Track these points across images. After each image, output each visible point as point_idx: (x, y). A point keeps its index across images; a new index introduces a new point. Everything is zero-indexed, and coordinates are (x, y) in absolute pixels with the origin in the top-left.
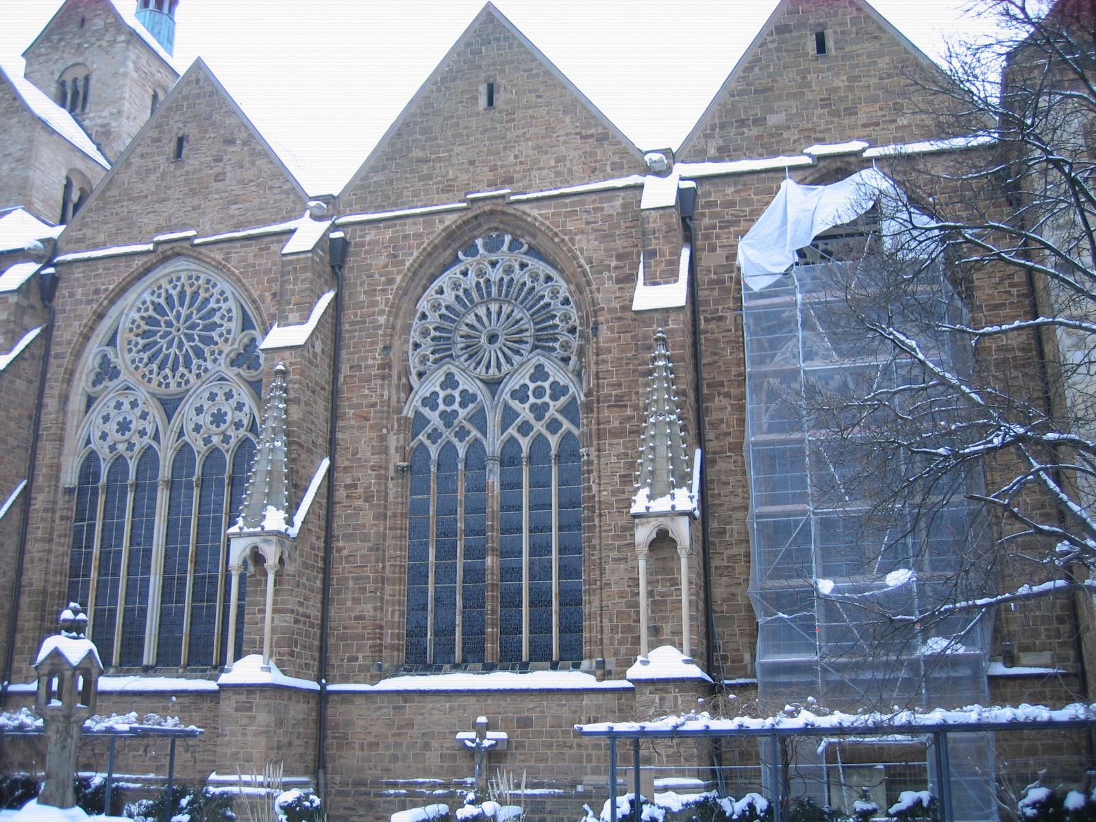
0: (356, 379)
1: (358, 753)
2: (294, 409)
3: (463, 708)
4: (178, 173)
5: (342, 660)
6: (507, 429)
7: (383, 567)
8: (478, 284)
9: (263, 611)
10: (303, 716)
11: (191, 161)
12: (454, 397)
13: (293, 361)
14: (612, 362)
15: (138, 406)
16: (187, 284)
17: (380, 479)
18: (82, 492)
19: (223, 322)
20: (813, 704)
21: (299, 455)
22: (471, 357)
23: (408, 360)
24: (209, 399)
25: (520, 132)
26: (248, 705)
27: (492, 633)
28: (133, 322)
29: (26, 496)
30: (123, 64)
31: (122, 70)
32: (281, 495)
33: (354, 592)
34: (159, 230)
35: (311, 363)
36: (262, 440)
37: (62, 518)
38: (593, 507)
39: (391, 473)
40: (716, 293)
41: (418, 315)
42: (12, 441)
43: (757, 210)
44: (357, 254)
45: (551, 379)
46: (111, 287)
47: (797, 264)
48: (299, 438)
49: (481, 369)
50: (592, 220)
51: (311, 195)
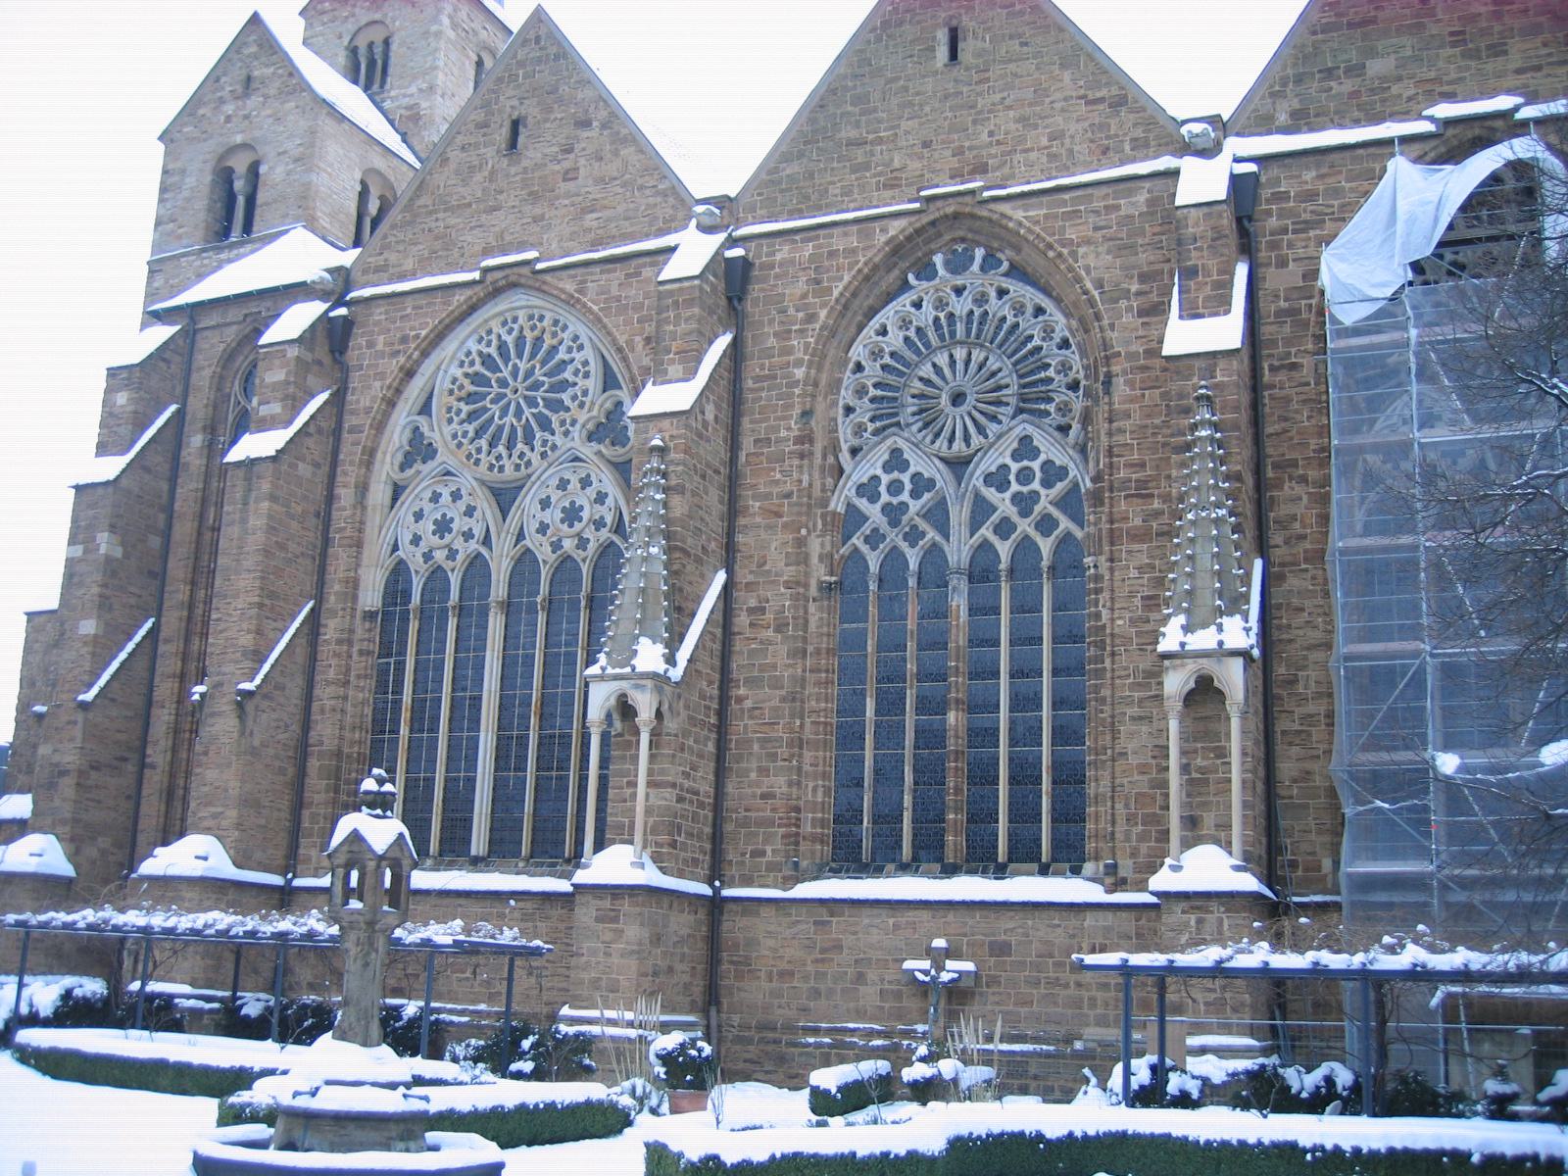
0: (763, 458)
1: (765, 985)
2: (676, 500)
3: (913, 926)
4: (513, 170)
5: (743, 854)
6: (850, 538)
7: (802, 726)
8: (937, 319)
9: (634, 784)
10: (689, 931)
11: (530, 153)
12: (901, 482)
13: (675, 432)
14: (1131, 432)
15: (461, 497)
16: (527, 326)
17: (797, 600)
18: (387, 616)
19: (577, 380)
20: (1425, 935)
21: (684, 566)
22: (926, 425)
23: (836, 431)
24: (558, 488)
25: (997, 97)
26: (613, 914)
27: (956, 821)
28: (454, 381)
29: (314, 622)
30: (435, 20)
31: (434, 28)
32: (658, 623)
33: (760, 759)
34: (487, 252)
35: (700, 436)
36: (632, 544)
37: (361, 653)
38: (1103, 642)
39: (813, 591)
40: (1287, 329)
41: (851, 365)
42: (292, 546)
43: (1349, 204)
44: (765, 279)
45: (1043, 457)
46: (424, 333)
47: (1411, 284)
48: (684, 542)
49: (941, 444)
50: (1102, 223)
51: (698, 196)
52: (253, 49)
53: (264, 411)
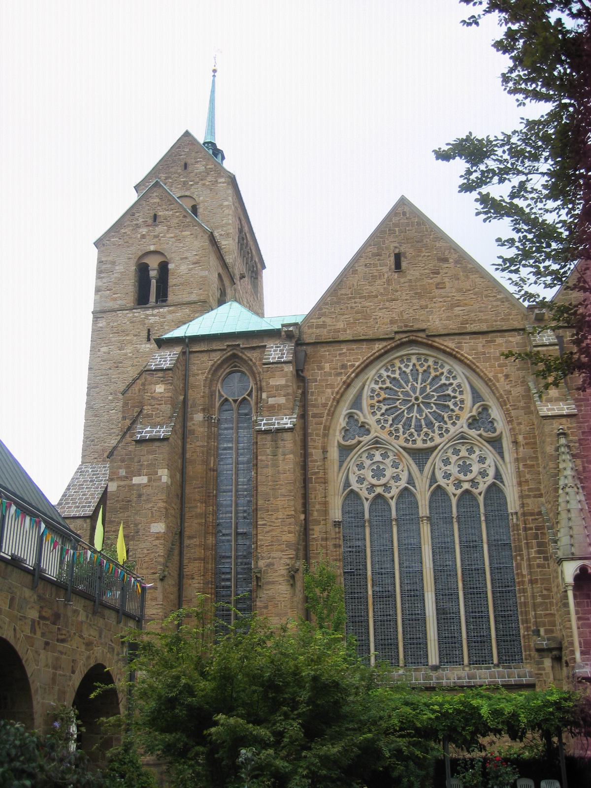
4: (402, 280)
11: (412, 272)
13: (570, 426)
31: (226, 203)
46: (357, 364)
52: (157, 200)
53: (271, 401)
